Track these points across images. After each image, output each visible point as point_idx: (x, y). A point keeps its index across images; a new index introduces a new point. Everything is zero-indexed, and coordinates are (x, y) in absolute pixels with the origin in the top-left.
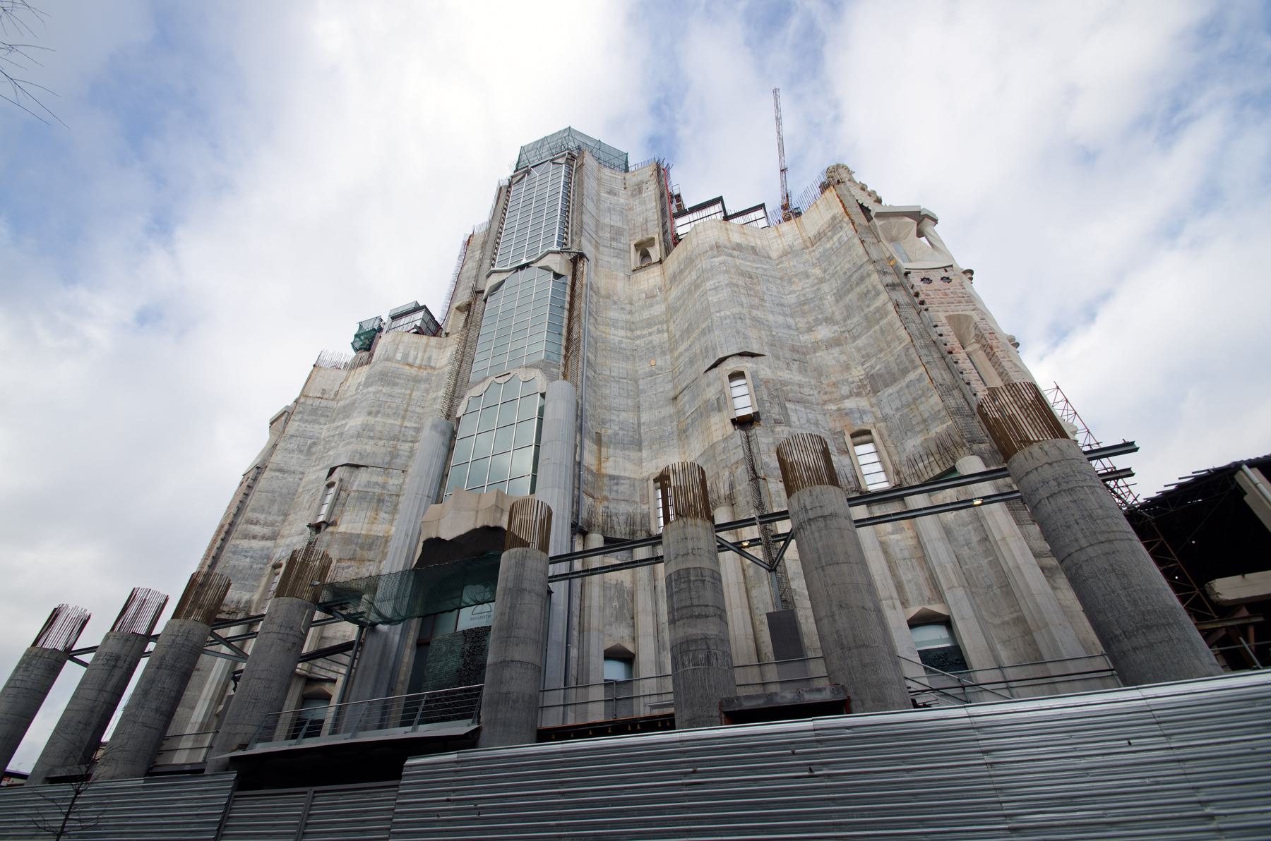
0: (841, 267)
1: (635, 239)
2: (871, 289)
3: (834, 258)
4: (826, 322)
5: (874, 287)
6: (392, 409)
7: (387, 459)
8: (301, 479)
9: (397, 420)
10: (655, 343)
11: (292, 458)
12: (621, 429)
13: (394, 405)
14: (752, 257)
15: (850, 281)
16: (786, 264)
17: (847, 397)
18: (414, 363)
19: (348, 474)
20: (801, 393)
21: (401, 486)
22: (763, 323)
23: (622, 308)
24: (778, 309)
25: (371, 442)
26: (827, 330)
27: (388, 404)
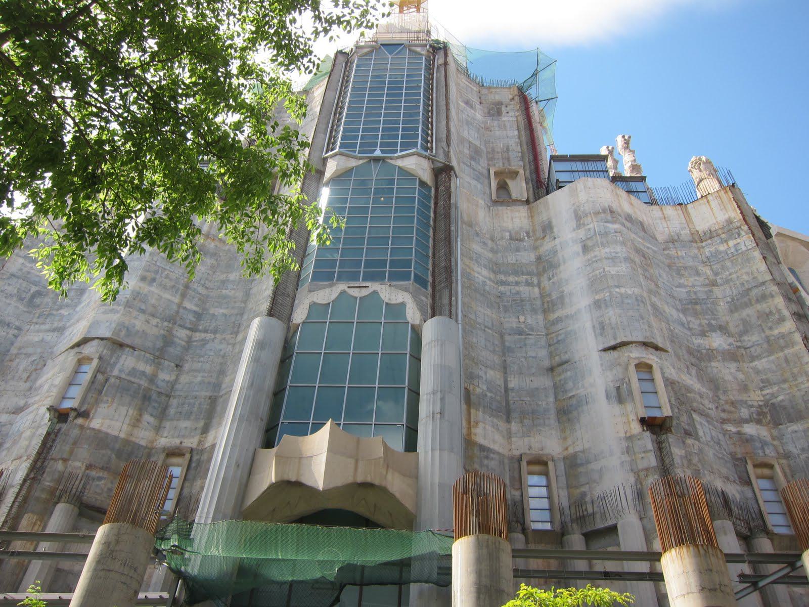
0: (738, 277)
1: (494, 165)
2: (774, 312)
3: (728, 264)
4: (720, 331)
5: (779, 311)
6: (171, 280)
7: (159, 344)
8: (16, 336)
9: (175, 297)
10: (523, 296)
11: (9, 304)
13: (173, 276)
14: (642, 234)
15: (748, 295)
16: (673, 252)
17: (747, 421)
19: (109, 353)
21: (173, 385)
23: (484, 243)
24: (670, 300)
25: (142, 317)
26: (721, 339)
27: (166, 272)
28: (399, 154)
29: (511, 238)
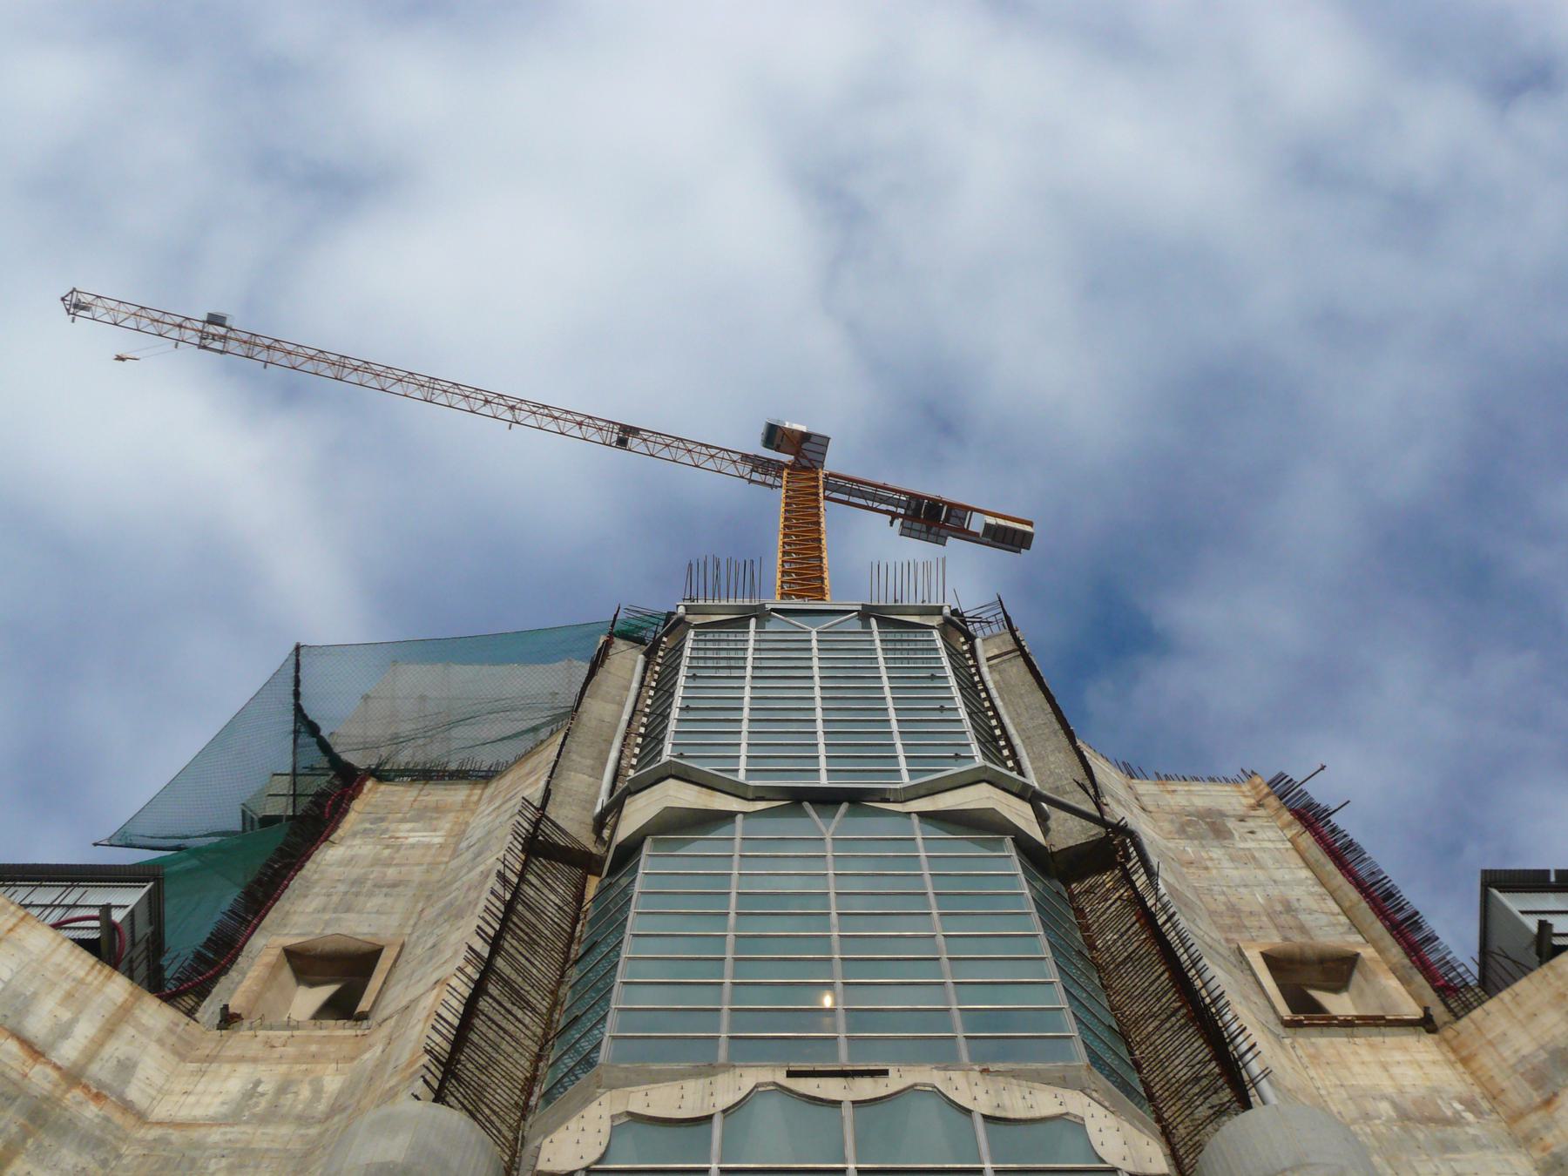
18: (52, 1046)
28: (906, 780)
29: (1404, 1116)
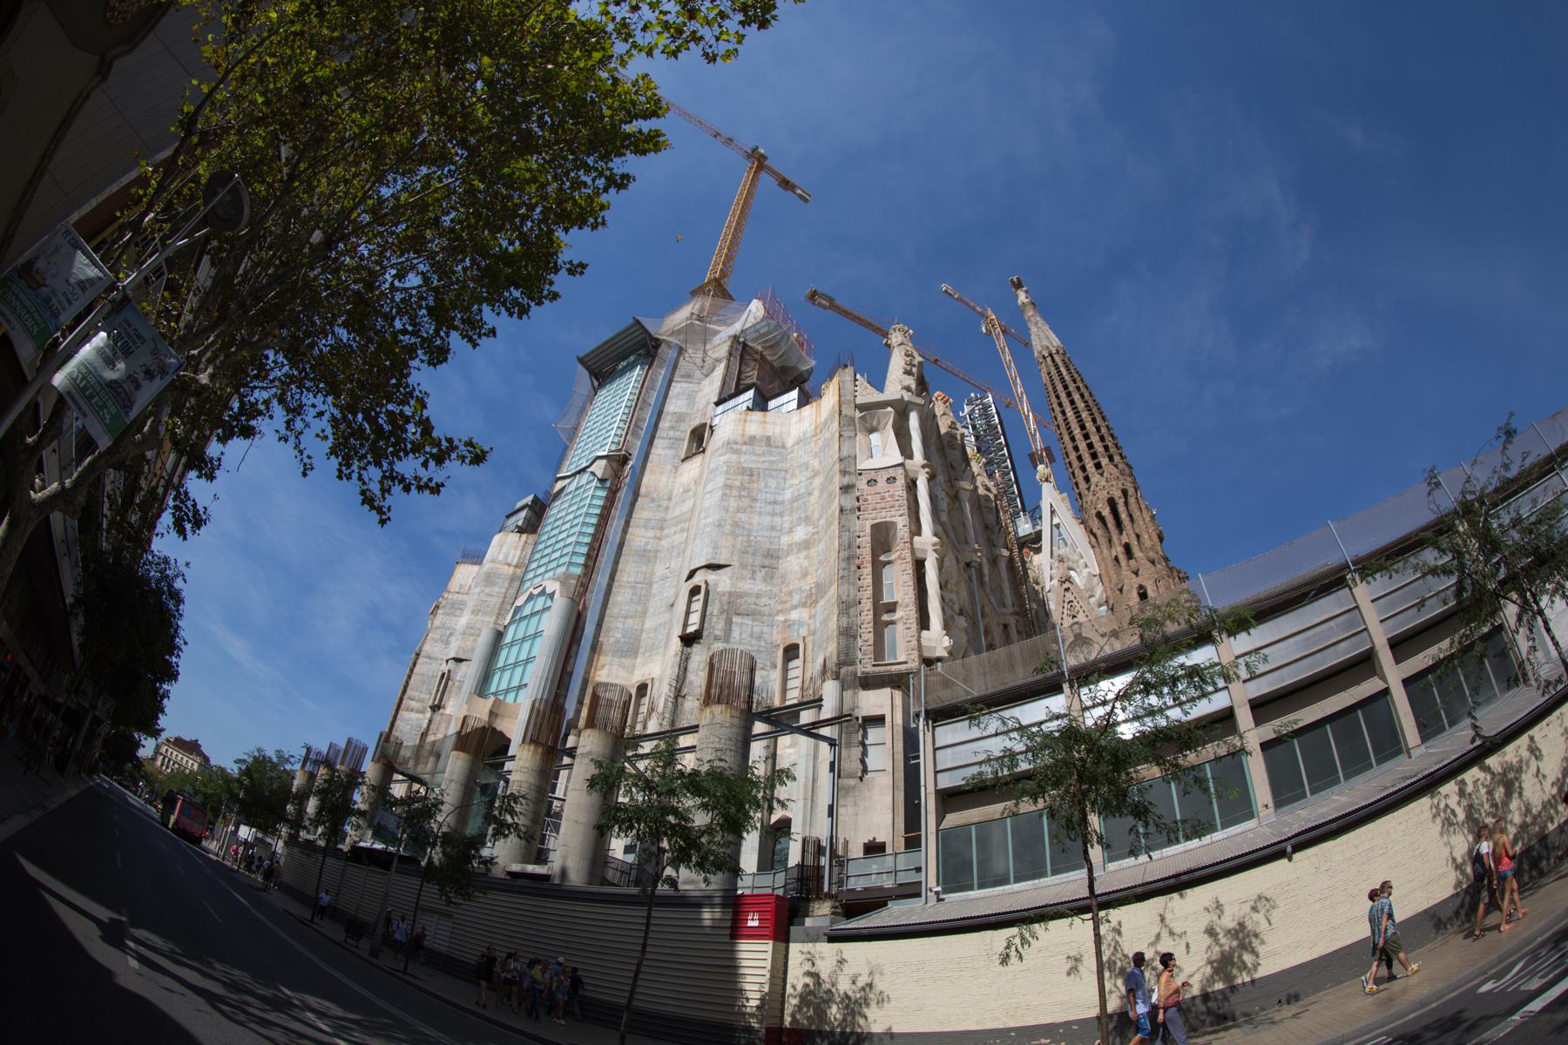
12: (623, 636)
17: (795, 607)
20: (755, 604)
22: (744, 528)
24: (769, 508)
